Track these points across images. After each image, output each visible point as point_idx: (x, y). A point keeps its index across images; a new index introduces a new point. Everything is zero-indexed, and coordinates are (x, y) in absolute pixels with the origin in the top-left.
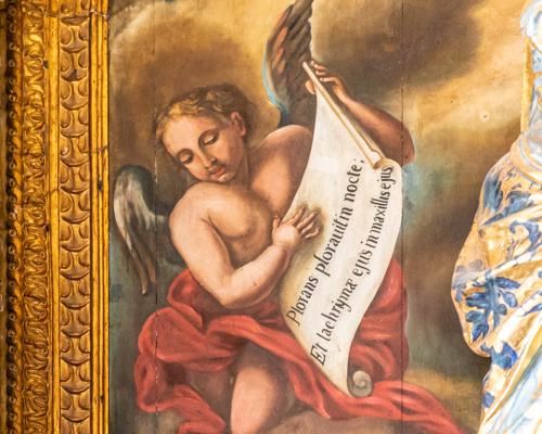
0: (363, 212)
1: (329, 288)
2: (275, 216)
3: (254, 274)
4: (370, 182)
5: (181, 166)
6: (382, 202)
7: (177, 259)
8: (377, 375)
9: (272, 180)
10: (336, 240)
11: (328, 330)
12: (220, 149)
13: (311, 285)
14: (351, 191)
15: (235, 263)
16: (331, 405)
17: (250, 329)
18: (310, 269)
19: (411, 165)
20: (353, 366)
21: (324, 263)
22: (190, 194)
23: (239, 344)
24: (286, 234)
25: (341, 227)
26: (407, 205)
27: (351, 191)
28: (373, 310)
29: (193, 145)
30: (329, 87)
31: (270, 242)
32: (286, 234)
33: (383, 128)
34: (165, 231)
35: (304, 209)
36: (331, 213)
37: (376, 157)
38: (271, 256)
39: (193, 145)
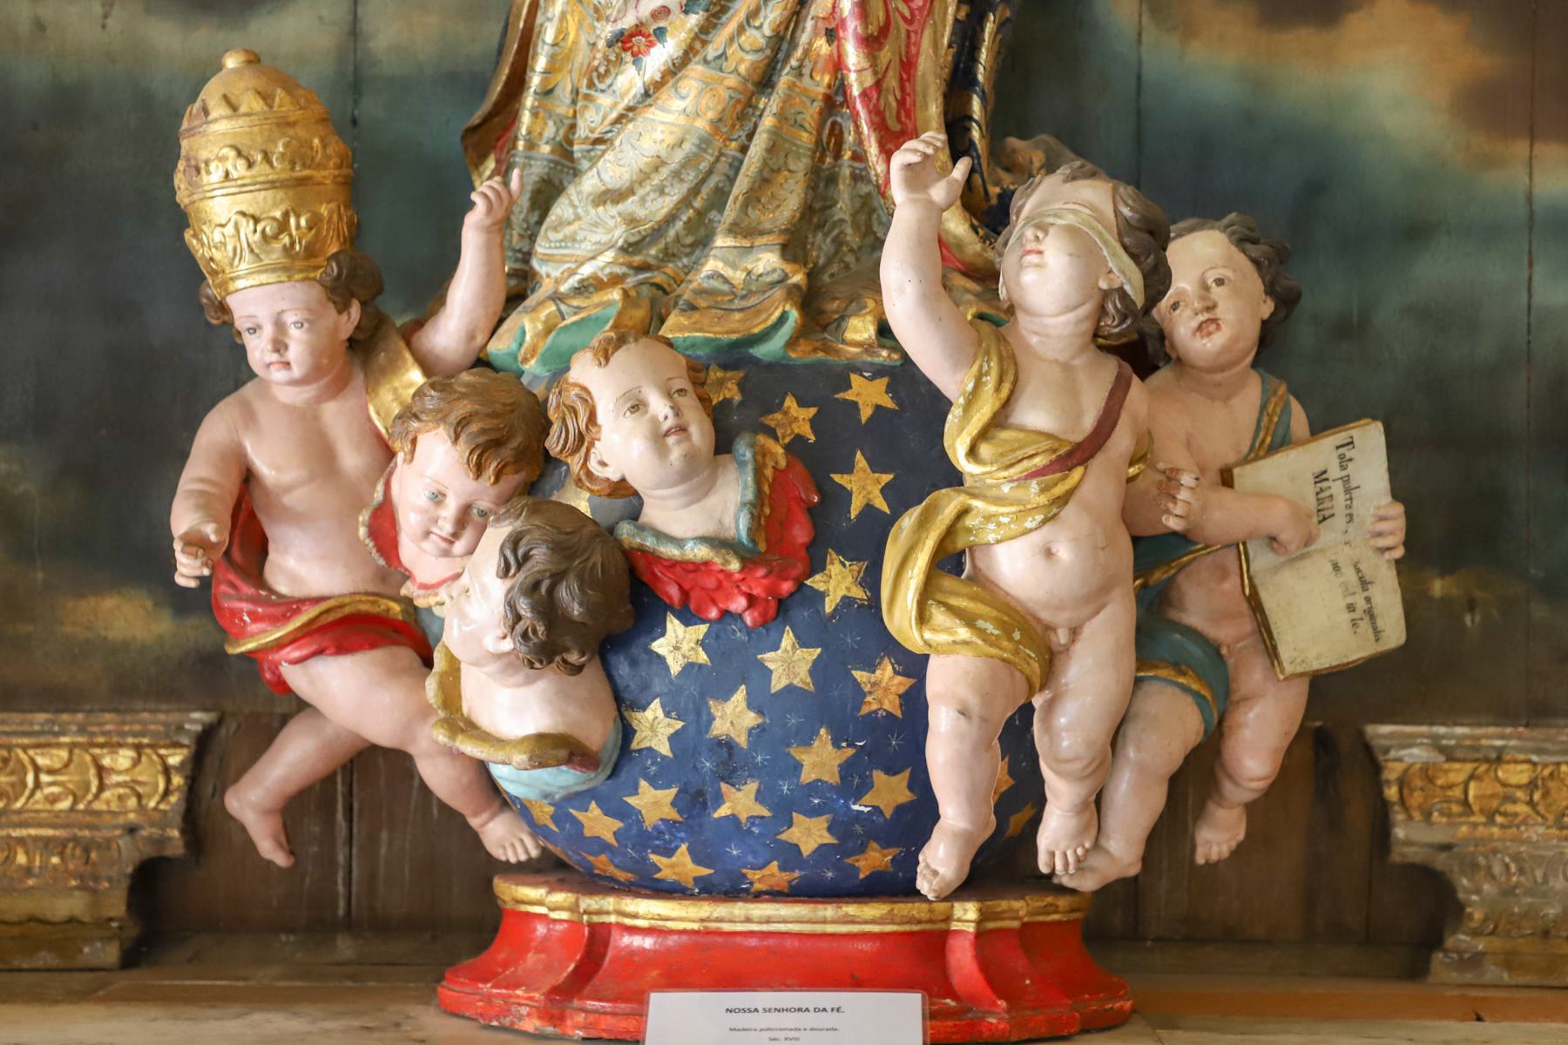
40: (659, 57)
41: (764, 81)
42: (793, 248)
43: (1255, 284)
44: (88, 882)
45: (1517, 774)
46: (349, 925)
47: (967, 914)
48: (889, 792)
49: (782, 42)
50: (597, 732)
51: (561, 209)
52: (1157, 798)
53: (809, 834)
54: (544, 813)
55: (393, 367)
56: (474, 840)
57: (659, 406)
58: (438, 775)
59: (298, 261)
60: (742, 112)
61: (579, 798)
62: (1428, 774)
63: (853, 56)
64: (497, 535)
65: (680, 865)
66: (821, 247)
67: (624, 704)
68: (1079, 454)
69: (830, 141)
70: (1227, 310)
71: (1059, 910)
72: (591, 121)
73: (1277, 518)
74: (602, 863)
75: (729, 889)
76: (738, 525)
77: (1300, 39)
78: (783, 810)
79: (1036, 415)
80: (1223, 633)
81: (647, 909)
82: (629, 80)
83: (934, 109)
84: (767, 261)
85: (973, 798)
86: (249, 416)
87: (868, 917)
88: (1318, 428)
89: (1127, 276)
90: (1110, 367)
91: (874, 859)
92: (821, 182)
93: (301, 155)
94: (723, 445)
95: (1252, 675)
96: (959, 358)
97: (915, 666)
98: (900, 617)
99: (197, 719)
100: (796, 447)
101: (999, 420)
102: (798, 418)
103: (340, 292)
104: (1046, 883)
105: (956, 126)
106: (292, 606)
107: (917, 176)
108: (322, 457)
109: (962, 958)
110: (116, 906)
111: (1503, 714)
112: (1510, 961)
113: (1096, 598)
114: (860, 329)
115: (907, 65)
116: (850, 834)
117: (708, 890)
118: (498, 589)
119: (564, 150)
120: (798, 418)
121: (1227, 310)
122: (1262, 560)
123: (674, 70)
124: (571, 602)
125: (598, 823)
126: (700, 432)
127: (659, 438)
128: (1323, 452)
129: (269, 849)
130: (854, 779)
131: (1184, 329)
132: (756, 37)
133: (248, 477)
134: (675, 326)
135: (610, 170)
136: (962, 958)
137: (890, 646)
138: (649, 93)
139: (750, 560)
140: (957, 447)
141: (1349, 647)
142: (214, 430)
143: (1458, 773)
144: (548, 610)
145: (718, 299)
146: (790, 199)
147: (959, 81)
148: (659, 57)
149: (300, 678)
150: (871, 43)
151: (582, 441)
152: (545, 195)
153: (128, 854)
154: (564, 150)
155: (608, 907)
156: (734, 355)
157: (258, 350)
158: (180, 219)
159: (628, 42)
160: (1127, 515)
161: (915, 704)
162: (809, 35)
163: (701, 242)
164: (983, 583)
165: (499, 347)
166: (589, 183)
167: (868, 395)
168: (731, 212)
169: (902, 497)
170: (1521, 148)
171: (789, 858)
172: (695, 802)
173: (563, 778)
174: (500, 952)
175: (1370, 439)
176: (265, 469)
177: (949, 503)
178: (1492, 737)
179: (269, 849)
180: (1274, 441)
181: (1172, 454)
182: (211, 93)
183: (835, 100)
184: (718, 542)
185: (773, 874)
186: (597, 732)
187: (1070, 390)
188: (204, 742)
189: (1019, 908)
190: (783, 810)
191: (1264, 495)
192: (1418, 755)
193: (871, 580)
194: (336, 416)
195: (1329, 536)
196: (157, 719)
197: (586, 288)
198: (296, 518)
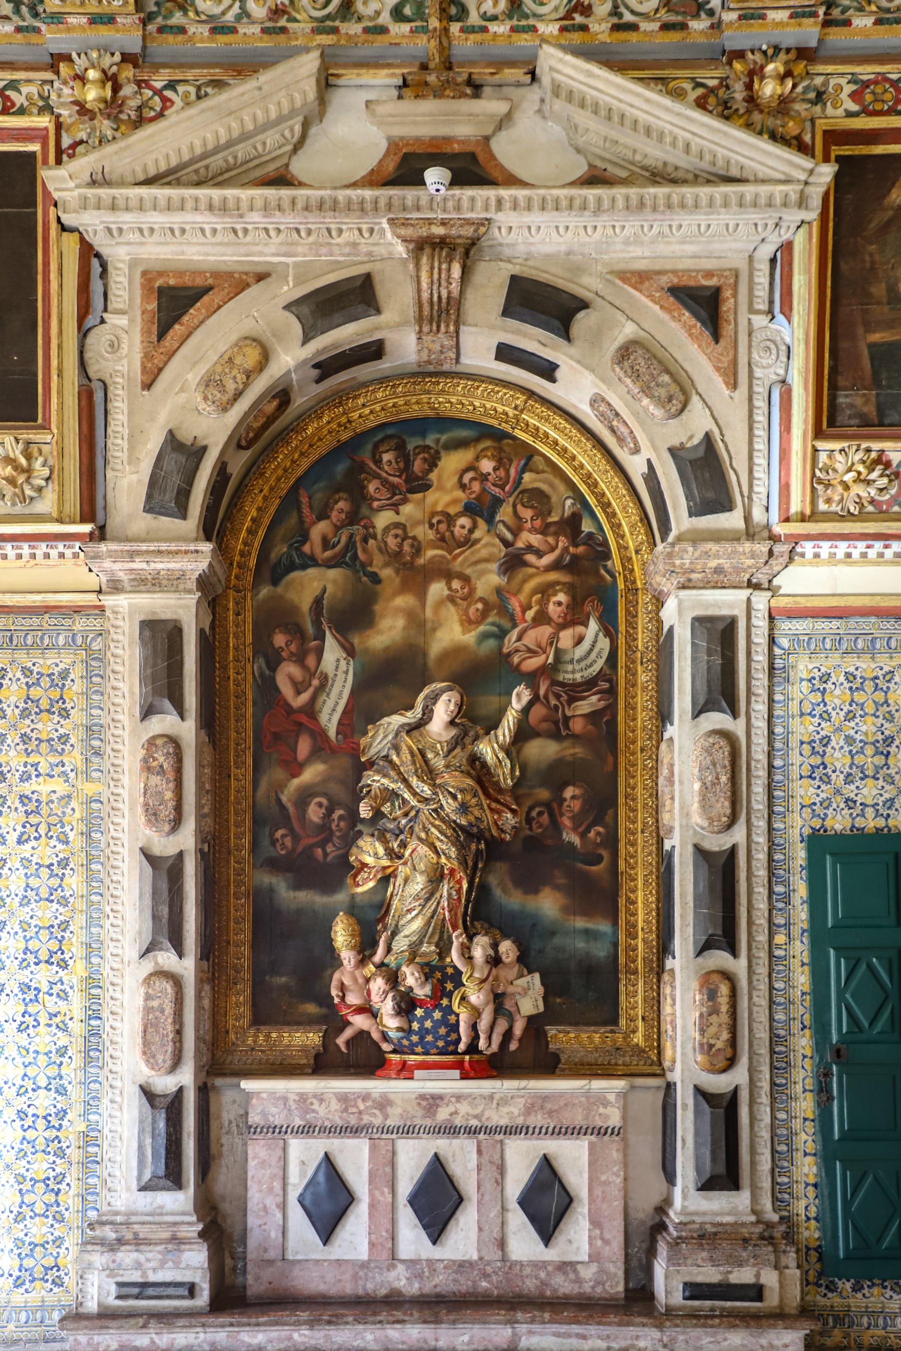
0: (341, 676)
1: (330, 703)
2: (312, 675)
3: (305, 697)
4: (343, 663)
5: (279, 654)
6: (346, 672)
7: (277, 690)
8: (345, 737)
9: (311, 661)
10: (332, 686)
11: (330, 719)
12: (293, 647)
13: (324, 702)
14: (337, 668)
15: (298, 693)
16: (331, 748)
17: (304, 719)
18: (324, 697)
19: (357, 658)
20: (338, 733)
21: (328, 694)
22: (283, 664)
23: (300, 725)
24: (316, 682)
25: (334, 681)
26: (354, 674)
27: (337, 668)
28: (345, 712)
29: (283, 645)
30: (330, 628)
31: (310, 685)
32: (316, 682)
33: (347, 645)
34: (273, 679)
35: (322, 673)
36: (331, 675)
37: (344, 655)
38: (311, 690)
39: (283, 645)
40: (414, 913)
41: (432, 917)
42: (437, 946)
43: (516, 949)
44: (307, 1057)
45: (572, 1035)
46: (353, 1066)
47: (467, 1058)
48: (454, 1036)
49: (435, 911)
50: (406, 1027)
51: (397, 938)
52: (501, 1038)
53: (441, 1044)
54: (396, 1041)
55: (367, 964)
56: (380, 1048)
57: (417, 974)
58: (375, 1036)
59: (353, 948)
60: (428, 923)
61: (402, 1038)
62: (556, 1035)
63: (447, 914)
64: (390, 995)
65: (419, 1049)
66: (442, 944)
67: (410, 1022)
68: (483, 981)
69: (443, 926)
70: (511, 955)
71: (484, 1058)
72: (402, 922)
73: (519, 990)
74: (406, 1050)
75: (426, 1053)
76: (429, 993)
77: (531, 897)
78: (437, 1039)
79: (477, 975)
80: (512, 1009)
81: (413, 1057)
82: (409, 917)
83: (460, 922)
84: (433, 948)
85: (467, 1036)
86: (343, 973)
87: (450, 1058)
88: (530, 972)
89: (492, 952)
90: (489, 967)
91: (451, 1048)
92: (442, 933)
93: (353, 930)
94: (427, 980)
95: (517, 1017)
96: (464, 966)
97: (458, 1015)
98: (455, 1007)
99: (324, 1027)
100: (438, 980)
101: (471, 976)
102: (438, 975)
103: (359, 953)
104: (481, 1052)
105: (465, 922)
106: (351, 1006)
107: (457, 937)
108: (355, 980)
109: (467, 1065)
110: (312, 1062)
111: (570, 1024)
112: (570, 1069)
113: (487, 1004)
114: (448, 960)
115: (456, 914)
116: (448, 1043)
117: (424, 1054)
118: (391, 1003)
119: (397, 926)
120: (438, 975)
121: (511, 955)
122: (518, 997)
123: (417, 915)
124: (403, 1005)
125: (405, 1042)
126: (423, 978)
127: (416, 979)
128: (528, 978)
129: (344, 1049)
130: (448, 1034)
131: (504, 957)
132: (431, 910)
133: (342, 984)
134: (417, 960)
135: (406, 932)
136: (467, 1065)
137: (454, 1013)
138: (413, 918)
139: (431, 998)
140: (464, 981)
141: (534, 1012)
142: (336, 976)
143: (561, 1035)
144: (399, 1007)
145: (425, 954)
146: (436, 938)
147: (465, 914)
148: (414, 913)
149: (350, 1018)
150: (450, 911)
151: (404, 980)
152: (394, 934)
153: (313, 1052)
154: (397, 926)
155: (406, 1057)
156: (427, 964)
157: (345, 962)
158: (332, 940)
159: (409, 911)
160: (492, 991)
161: (458, 1021)
162: (440, 910)
163: (421, 943)
164: (468, 1002)
165: (386, 961)
166: (402, 934)
167: (450, 971)
168: (426, 939)
169: (456, 988)
170: (572, 917)
171: (437, 1047)
172: (422, 1038)
173: (400, 1034)
174: (386, 1066)
175: (537, 976)
176: (346, 982)
177: (463, 989)
178: (568, 1028)
179: (344, 1049)
180: (520, 976)
181: (502, 979)
182: (338, 919)
183: (444, 919)
184: (426, 996)
185: (435, 1051)
186: (406, 1027)
187: (482, 971)
188: (326, 1031)
189: (476, 1057)
190: (437, 1039)
191: (517, 986)
192: (554, 1032)
193: (450, 1001)
194: (357, 973)
195: (530, 992)
196: (317, 1027)
197: (402, 952)
198: (351, 991)
